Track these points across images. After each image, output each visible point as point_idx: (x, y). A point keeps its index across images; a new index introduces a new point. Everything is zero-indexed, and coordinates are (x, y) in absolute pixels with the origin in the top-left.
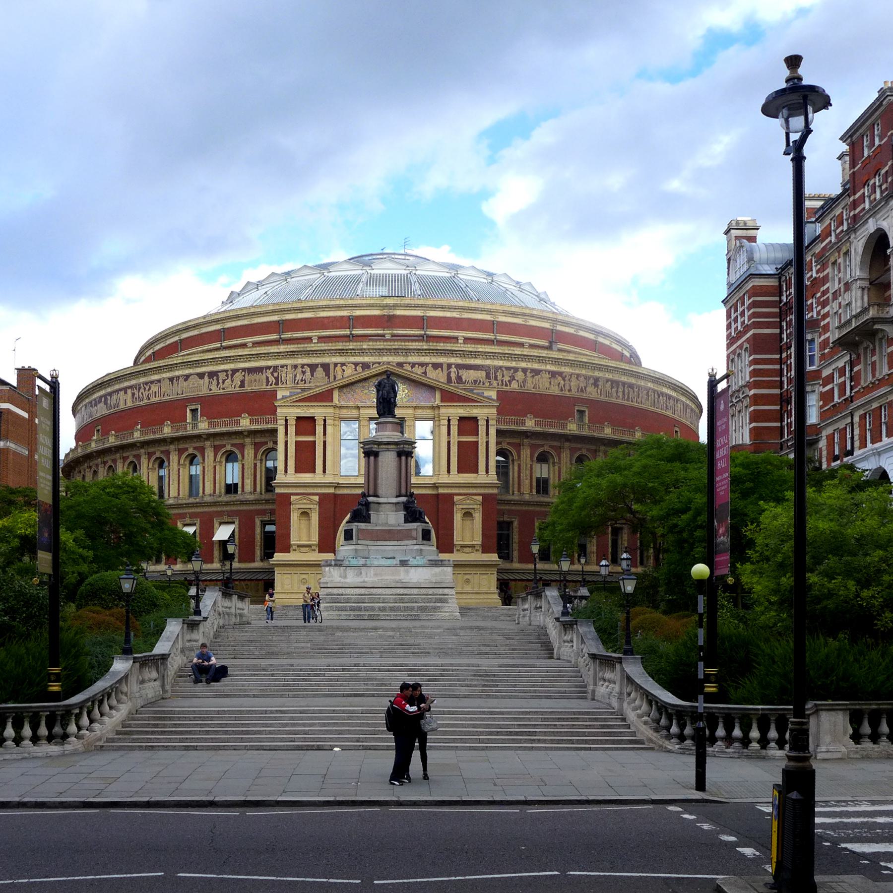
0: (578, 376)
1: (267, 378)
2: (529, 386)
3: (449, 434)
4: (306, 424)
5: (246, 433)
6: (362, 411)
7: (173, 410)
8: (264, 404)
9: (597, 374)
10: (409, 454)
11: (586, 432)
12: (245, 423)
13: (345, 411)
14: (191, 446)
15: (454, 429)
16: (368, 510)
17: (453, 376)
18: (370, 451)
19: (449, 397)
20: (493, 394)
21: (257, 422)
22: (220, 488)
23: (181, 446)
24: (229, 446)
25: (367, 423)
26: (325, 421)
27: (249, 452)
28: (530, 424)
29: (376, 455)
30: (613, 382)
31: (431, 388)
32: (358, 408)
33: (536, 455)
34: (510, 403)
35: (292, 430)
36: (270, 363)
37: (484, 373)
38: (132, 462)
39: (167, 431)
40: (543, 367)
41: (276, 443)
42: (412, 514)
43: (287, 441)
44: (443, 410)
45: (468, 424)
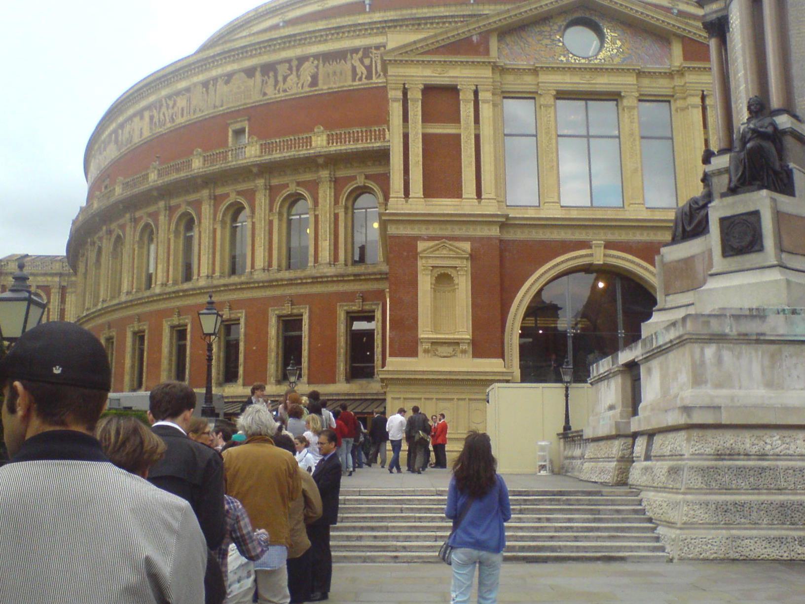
1: (354, 68)
4: (441, 100)
5: (321, 161)
6: (543, 78)
12: (320, 142)
13: (509, 78)
21: (339, 139)
23: (219, 191)
25: (551, 100)
26: (476, 93)
27: (326, 193)
32: (535, 71)
35: (416, 111)
36: (358, 43)
38: (147, 225)
39: (197, 165)
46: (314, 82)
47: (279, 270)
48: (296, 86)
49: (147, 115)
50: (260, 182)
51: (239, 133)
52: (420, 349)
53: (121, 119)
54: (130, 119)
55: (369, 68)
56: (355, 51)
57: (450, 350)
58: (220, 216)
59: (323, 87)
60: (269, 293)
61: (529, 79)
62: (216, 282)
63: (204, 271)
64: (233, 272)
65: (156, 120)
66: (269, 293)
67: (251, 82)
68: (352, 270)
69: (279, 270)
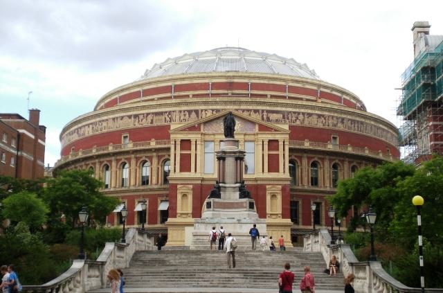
0: (333, 117)
2: (306, 123)
3: (263, 150)
4: (186, 144)
6: (216, 137)
7: (114, 137)
8: (162, 133)
9: (343, 116)
10: (241, 159)
11: (338, 149)
12: (153, 144)
13: (207, 136)
14: (122, 158)
15: (266, 147)
16: (219, 191)
17: (265, 117)
18: (221, 158)
19: (263, 128)
20: (286, 127)
21: (160, 143)
22: (139, 181)
23: (118, 158)
24: (141, 157)
27: (155, 161)
28: (307, 145)
29: (224, 159)
30: (352, 120)
31: (253, 123)
32: (214, 134)
33: (311, 163)
34: (297, 133)
35: (178, 147)
37: (282, 116)
39: (111, 149)
40: (313, 112)
41: (169, 156)
42: (244, 193)
43: (176, 153)
44: (259, 136)
45: (273, 144)
46: (152, 122)
47: (139, 186)
48: (146, 123)
49: (91, 126)
50: (133, 156)
51: (125, 137)
52: (177, 216)
53: (80, 125)
54: (84, 126)
55: (170, 119)
56: (166, 112)
57: (185, 216)
58: (118, 166)
59: (155, 124)
60: (135, 194)
61: (213, 136)
62: (117, 190)
63: (113, 185)
64: (123, 185)
65: (95, 128)
66: (135, 194)
67: (130, 120)
68: (163, 186)
69: (139, 186)
